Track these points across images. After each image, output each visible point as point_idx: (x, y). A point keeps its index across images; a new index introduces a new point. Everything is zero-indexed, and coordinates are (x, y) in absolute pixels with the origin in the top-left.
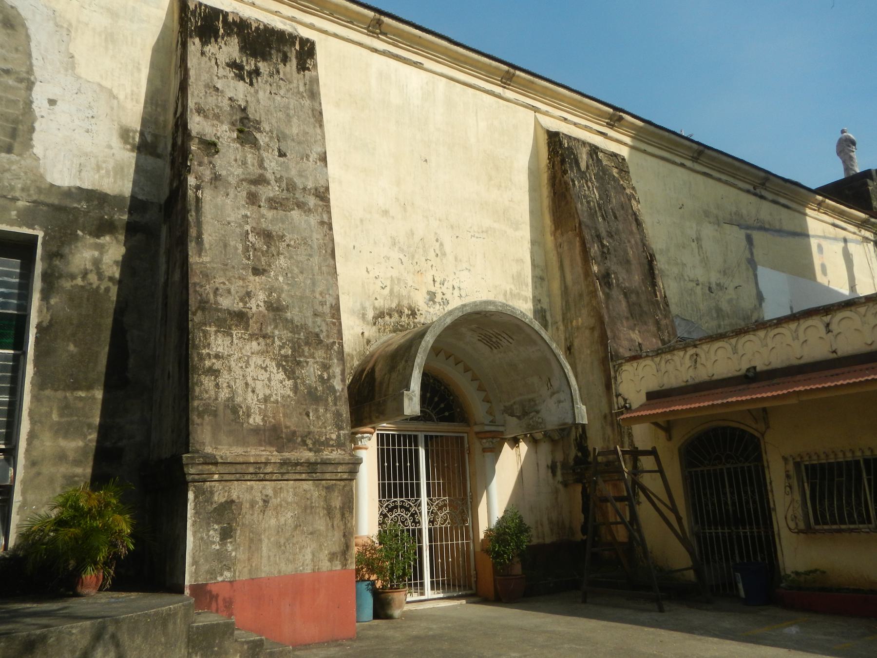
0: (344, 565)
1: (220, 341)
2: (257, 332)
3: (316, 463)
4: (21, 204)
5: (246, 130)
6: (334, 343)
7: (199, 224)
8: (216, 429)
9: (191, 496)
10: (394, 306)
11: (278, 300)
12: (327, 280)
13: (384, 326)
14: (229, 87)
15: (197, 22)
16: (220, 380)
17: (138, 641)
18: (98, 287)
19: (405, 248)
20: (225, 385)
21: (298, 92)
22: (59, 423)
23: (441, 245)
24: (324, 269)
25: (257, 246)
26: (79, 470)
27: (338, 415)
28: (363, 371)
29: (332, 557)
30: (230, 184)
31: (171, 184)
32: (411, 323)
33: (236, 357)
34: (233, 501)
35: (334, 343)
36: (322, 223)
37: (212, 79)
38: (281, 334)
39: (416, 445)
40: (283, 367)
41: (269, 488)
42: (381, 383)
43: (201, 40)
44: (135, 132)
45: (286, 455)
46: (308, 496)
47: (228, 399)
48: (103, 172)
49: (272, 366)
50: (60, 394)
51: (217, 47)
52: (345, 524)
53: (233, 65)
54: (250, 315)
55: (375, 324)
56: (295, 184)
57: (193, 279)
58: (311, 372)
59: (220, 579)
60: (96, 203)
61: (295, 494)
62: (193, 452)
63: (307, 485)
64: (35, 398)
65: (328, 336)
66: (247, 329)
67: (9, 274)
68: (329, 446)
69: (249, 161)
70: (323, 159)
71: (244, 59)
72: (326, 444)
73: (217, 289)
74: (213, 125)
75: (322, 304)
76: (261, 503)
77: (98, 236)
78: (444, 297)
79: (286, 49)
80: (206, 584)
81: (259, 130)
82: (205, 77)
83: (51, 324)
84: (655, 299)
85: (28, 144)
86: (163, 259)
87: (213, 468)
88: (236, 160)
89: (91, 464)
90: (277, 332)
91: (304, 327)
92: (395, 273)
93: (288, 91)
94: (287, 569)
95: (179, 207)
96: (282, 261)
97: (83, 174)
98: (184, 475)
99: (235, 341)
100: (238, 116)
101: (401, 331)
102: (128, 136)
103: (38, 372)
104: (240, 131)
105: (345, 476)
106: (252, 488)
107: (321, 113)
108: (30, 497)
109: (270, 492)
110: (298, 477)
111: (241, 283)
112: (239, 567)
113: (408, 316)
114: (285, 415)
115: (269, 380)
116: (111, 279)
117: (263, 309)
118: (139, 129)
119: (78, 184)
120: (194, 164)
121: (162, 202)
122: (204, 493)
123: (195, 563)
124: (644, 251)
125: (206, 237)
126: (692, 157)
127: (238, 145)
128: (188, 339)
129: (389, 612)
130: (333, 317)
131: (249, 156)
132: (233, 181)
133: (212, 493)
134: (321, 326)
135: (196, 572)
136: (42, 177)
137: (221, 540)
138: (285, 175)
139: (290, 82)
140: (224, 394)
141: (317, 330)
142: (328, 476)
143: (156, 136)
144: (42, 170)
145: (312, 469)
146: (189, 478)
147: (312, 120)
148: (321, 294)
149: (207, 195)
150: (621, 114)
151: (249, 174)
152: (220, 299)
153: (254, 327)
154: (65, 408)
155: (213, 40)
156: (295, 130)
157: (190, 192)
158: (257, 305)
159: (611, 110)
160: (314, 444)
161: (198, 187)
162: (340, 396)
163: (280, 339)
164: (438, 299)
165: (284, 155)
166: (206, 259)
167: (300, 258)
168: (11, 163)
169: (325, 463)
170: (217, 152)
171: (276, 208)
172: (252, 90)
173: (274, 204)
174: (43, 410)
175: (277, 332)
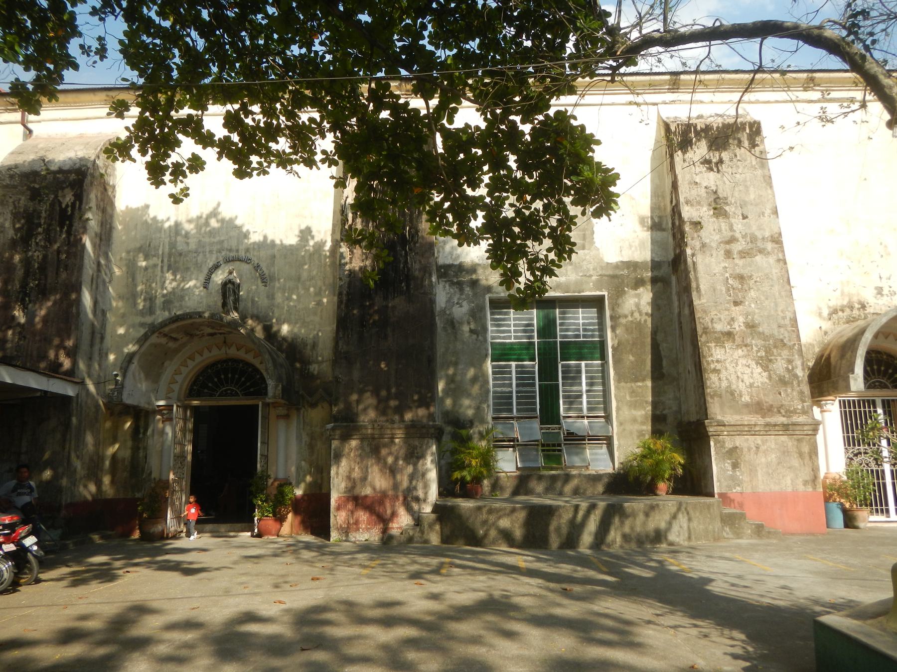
0: (815, 488)
1: (718, 352)
2: (740, 343)
3: (788, 425)
4: (594, 278)
5: (719, 206)
6: (795, 344)
7: (697, 279)
8: (722, 406)
9: (712, 443)
10: (845, 303)
11: (753, 320)
12: (786, 301)
13: (838, 319)
14: (704, 178)
15: (678, 140)
16: (721, 376)
17: (698, 514)
18: (640, 320)
20: (724, 378)
21: (752, 166)
22: (630, 401)
23: (886, 246)
24: (783, 293)
25: (735, 286)
26: (644, 428)
27: (801, 393)
28: (822, 356)
29: (805, 483)
30: (712, 247)
31: (675, 249)
32: (862, 314)
33: (729, 360)
34: (737, 447)
35: (795, 344)
36: (779, 260)
37: (692, 177)
38: (756, 342)
39: (875, 407)
40: (760, 364)
41: (759, 439)
42: (835, 367)
43: (682, 152)
44: (647, 218)
45: (768, 420)
46: (785, 445)
47: (727, 387)
48: (633, 249)
49: (753, 364)
50: (629, 385)
51: (693, 152)
52: (813, 463)
53: (706, 162)
54: (735, 333)
55: (830, 319)
56: (756, 236)
57: (698, 315)
58: (780, 366)
59: (734, 491)
60: (632, 269)
61: (776, 444)
62: (710, 419)
63: (784, 438)
64: (617, 388)
65: (790, 340)
66: (734, 342)
67: (592, 318)
68: (796, 413)
69: (723, 228)
70: (775, 212)
71: (711, 154)
72: (795, 412)
73: (713, 319)
74: (697, 210)
75: (784, 318)
76: (754, 449)
77: (636, 289)
78: (891, 289)
79: (739, 135)
80: (726, 493)
81: (727, 204)
82: (688, 177)
83: (619, 344)
85: (592, 242)
86: (675, 298)
87: (723, 428)
88: (714, 230)
89: (650, 424)
90: (754, 342)
91: (772, 336)
93: (744, 168)
94: (776, 488)
95: (682, 267)
96: (752, 294)
97: (623, 252)
98: (707, 432)
99: (728, 351)
100: (713, 197)
101: (853, 321)
102: (644, 221)
103: (616, 373)
104: (715, 209)
105: (810, 433)
106: (748, 440)
107: (770, 177)
108: (622, 442)
109: (759, 442)
110: (777, 433)
111: (727, 313)
112: (745, 485)
113: (859, 309)
114: (764, 395)
115: (752, 373)
116: (647, 314)
117: (743, 328)
118: (649, 215)
119: (621, 259)
120: (688, 240)
121: (670, 260)
122: (719, 442)
123: (719, 481)
125: (702, 287)
127: (715, 219)
128: (699, 353)
129: (856, 524)
130: (792, 326)
131: (723, 225)
132: (714, 245)
133: (724, 442)
134: (784, 334)
135: (720, 486)
136: (602, 260)
137: (733, 469)
138: (748, 232)
139: (745, 161)
140: (724, 384)
141: (781, 337)
142: (797, 433)
143: (660, 217)
144: (601, 256)
145: (786, 428)
146: (710, 434)
147: (764, 184)
148: (782, 311)
149: (699, 259)
151: (724, 237)
152: (715, 325)
153: (738, 340)
154: (633, 392)
155: (689, 148)
156: (752, 197)
157: (689, 260)
158: (739, 326)
160: (786, 412)
161: (693, 255)
162: (802, 380)
163: (756, 346)
164: (885, 292)
165: (747, 217)
166: (704, 301)
167: (764, 289)
168: (585, 255)
169: (794, 424)
170: (702, 228)
171: (745, 257)
172: (719, 176)
173: (743, 254)
174: (622, 394)
175: (754, 342)
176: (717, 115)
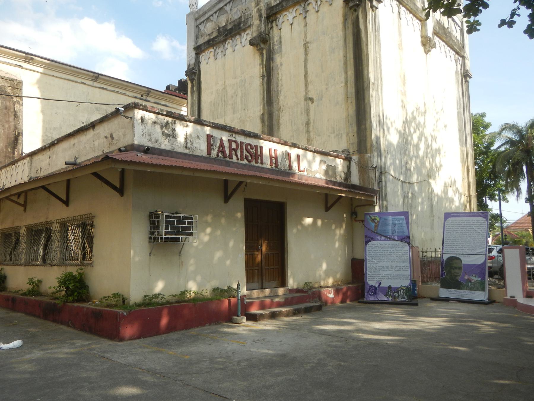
84: (12, 155)
124: (15, 130)
126: (92, 79)
150: (32, 56)
159: (24, 55)
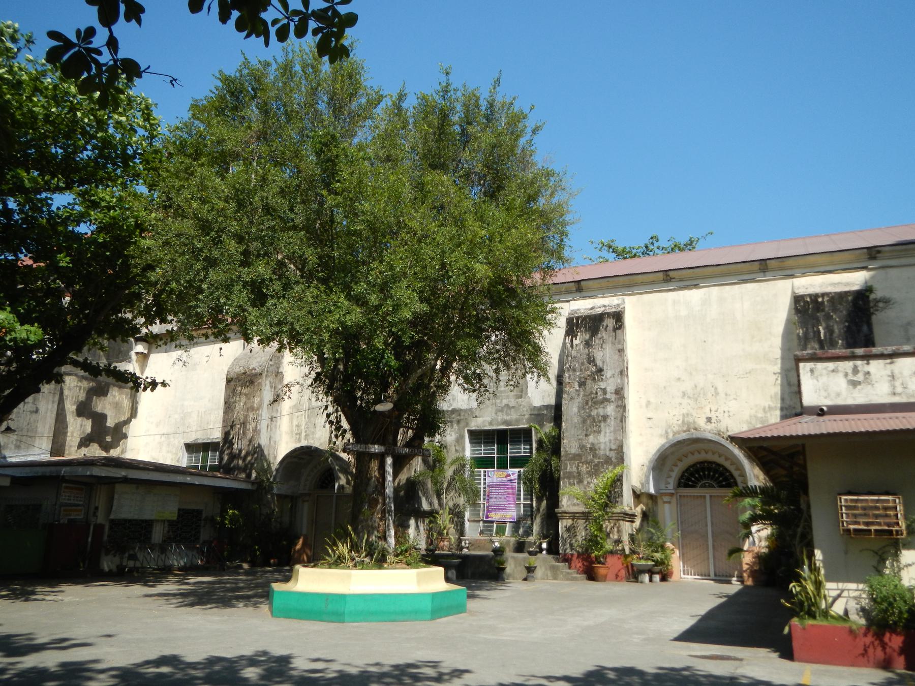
19: (691, 396)
23: (716, 389)
92: (685, 411)
134: (613, 455)
164: (713, 420)
176: (605, 306)
